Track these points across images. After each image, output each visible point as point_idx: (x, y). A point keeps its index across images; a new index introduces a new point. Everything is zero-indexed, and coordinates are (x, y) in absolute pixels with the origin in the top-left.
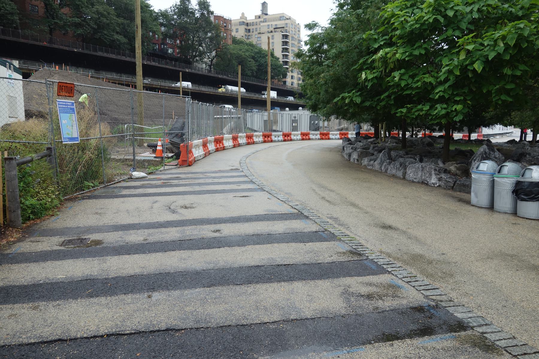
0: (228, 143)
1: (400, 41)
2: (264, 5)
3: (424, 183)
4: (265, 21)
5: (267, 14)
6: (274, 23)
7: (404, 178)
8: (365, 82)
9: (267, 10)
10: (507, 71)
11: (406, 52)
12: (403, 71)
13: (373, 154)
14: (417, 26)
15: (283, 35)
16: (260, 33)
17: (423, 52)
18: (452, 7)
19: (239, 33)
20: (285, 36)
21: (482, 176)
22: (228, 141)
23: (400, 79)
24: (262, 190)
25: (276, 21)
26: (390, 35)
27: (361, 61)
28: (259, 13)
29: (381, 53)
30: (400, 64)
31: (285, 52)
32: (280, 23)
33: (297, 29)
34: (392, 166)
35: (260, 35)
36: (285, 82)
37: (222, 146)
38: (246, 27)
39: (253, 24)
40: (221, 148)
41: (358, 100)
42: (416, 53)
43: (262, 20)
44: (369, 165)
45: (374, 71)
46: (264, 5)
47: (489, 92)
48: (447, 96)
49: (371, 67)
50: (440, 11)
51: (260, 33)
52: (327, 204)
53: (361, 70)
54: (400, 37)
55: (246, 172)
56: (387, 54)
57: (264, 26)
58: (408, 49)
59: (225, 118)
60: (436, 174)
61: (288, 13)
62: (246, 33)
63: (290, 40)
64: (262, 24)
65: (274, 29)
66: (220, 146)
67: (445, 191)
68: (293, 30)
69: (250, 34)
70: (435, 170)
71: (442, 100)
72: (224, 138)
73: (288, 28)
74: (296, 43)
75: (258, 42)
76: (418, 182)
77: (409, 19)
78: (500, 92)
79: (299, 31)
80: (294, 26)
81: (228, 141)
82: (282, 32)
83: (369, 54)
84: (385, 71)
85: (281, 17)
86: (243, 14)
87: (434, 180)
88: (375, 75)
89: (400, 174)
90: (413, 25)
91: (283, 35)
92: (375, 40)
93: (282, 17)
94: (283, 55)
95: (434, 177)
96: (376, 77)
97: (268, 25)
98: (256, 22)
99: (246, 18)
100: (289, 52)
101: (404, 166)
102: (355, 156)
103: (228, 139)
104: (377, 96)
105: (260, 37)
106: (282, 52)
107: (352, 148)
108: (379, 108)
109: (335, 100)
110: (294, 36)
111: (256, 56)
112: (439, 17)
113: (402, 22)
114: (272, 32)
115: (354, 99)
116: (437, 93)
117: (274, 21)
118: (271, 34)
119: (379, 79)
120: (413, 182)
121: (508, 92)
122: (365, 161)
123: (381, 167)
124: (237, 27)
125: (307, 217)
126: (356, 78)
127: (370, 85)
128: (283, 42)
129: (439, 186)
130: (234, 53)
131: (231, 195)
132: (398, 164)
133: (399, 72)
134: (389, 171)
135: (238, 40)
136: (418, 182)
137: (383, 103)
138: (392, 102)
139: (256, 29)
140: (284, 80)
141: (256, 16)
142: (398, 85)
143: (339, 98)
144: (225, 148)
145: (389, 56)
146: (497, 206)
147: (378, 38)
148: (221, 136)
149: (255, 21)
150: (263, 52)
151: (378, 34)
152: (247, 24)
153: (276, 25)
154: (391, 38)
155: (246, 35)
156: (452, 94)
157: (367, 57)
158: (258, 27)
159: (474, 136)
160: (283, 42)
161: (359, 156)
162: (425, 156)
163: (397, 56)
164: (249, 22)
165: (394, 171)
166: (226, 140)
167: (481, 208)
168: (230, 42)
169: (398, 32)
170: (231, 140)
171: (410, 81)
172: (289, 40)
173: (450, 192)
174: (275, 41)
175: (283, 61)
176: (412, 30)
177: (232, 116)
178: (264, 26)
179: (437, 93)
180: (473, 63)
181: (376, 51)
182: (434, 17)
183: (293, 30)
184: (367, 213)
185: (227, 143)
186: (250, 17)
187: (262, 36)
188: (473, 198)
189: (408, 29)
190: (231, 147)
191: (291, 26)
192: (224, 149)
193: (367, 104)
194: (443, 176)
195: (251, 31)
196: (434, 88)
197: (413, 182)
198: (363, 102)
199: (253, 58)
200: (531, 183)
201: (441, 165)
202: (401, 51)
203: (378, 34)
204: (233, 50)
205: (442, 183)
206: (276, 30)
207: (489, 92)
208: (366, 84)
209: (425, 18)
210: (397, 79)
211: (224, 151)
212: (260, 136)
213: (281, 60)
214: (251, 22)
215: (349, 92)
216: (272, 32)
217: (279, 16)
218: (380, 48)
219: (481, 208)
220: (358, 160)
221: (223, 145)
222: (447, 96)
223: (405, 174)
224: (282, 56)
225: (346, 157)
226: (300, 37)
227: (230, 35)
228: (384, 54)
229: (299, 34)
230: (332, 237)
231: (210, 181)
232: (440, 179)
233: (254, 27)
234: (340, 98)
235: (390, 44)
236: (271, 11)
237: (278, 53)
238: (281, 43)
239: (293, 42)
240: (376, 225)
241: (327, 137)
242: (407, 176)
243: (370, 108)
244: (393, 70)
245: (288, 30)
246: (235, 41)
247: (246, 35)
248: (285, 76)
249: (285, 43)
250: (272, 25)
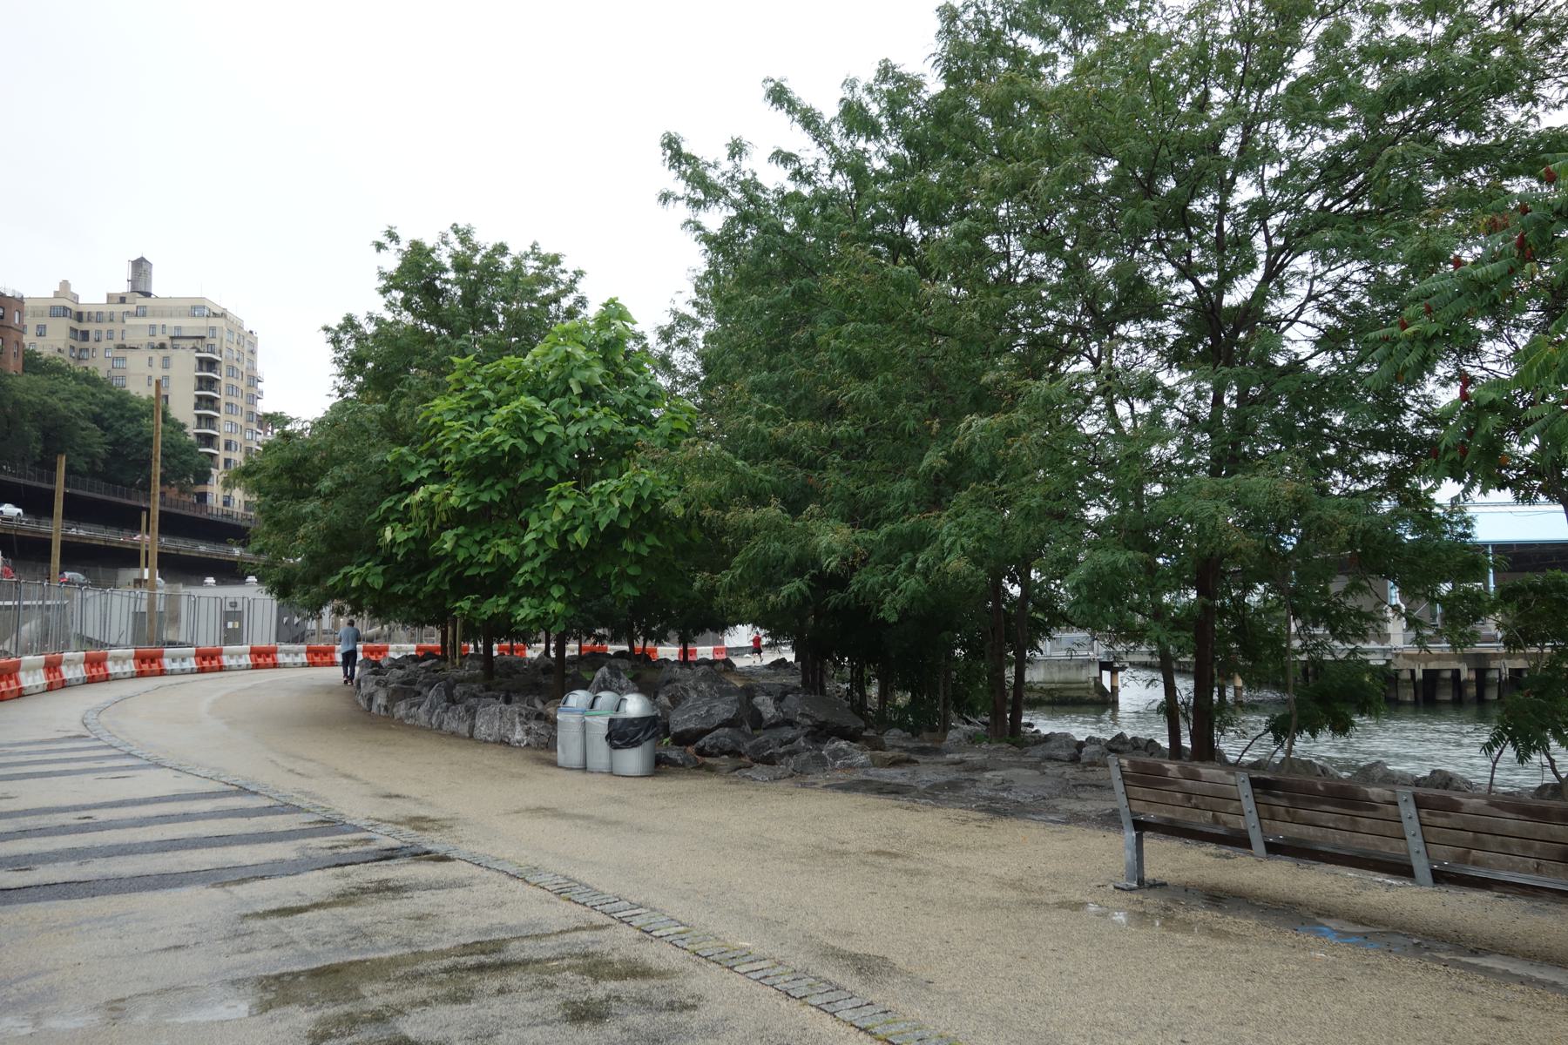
0: (32, 679)
1: (458, 473)
3: (504, 742)
4: (141, 313)
5: (148, 295)
6: (172, 323)
7: (471, 736)
8: (392, 547)
9: (148, 281)
10: (628, 545)
11: (467, 495)
12: (461, 530)
13: (419, 694)
14: (484, 450)
15: (201, 360)
16: (123, 347)
17: (497, 498)
18: (542, 427)
19: (52, 342)
20: (211, 364)
21: (569, 716)
22: (120, 662)
23: (457, 545)
24: (158, 765)
25: (180, 316)
26: (441, 460)
27: (385, 506)
28: (123, 287)
29: (420, 494)
30: (458, 517)
31: (206, 408)
32: (191, 325)
33: (247, 347)
34: (450, 714)
35: (121, 353)
36: (203, 497)
37: (14, 687)
38: (75, 324)
39: (99, 317)
40: (12, 691)
41: (377, 582)
42: (485, 497)
43: (132, 308)
44: (408, 717)
45: (410, 526)
47: (607, 577)
48: (536, 583)
49: (404, 518)
50: (522, 431)
51: (123, 347)
52: (297, 777)
53: (384, 521)
54: (458, 466)
55: (107, 740)
56: (432, 494)
58: (472, 490)
59: (26, 607)
60: (522, 723)
61: (220, 299)
62: (73, 343)
63: (224, 374)
64: (130, 321)
65: (172, 338)
66: (8, 686)
67: (530, 752)
68: (234, 347)
69: (90, 344)
70: (521, 715)
71: (528, 589)
72: (22, 665)
73: (216, 342)
74: (242, 385)
75: (115, 373)
76: (495, 742)
77: (471, 437)
78: (622, 576)
79: (252, 352)
80: (236, 337)
81: (120, 662)
82: (199, 351)
83: (400, 490)
84: (431, 526)
85: (194, 308)
86: (65, 285)
87: (518, 735)
88: (412, 534)
89: (464, 729)
90: (477, 447)
91: (201, 360)
92: (412, 467)
93: (197, 309)
94: (199, 417)
95: (518, 728)
96: (413, 538)
97: (153, 327)
98: (112, 314)
99: (77, 297)
100: (218, 410)
101: (472, 712)
102: (381, 699)
103: (32, 669)
104: (419, 572)
105: (124, 359)
106: (197, 407)
107: (378, 683)
108: (421, 596)
109: (331, 582)
110: (236, 364)
111: (106, 415)
112: (520, 442)
113: (457, 440)
114: (162, 346)
115: (369, 580)
116: (522, 575)
117: (171, 316)
118: (162, 352)
119: (422, 542)
120: (486, 741)
121: (632, 580)
122: (401, 709)
123: (430, 719)
124: (41, 321)
125: (256, 793)
126: (375, 535)
127: (401, 552)
128: (200, 379)
129: (528, 745)
130: (29, 401)
131: (90, 777)
132: (461, 708)
133: (455, 531)
134: (445, 727)
135: (46, 362)
136: (495, 742)
137: (428, 589)
138: (447, 587)
139: (110, 332)
140: (200, 488)
141: (110, 297)
142: (451, 556)
143: (337, 578)
144: (24, 692)
145: (436, 499)
146: (589, 765)
147: (418, 462)
148: (14, 659)
150: (132, 405)
151: (420, 455)
152: (79, 317)
153: (178, 328)
154: (443, 465)
155: (72, 348)
156: (547, 578)
157: (395, 498)
159: (704, 651)
160: (200, 379)
161: (389, 699)
162: (515, 692)
163: (452, 500)
164: (85, 310)
165: (454, 725)
166: (27, 670)
167: (572, 769)
168: (13, 365)
169: (451, 458)
170: (42, 672)
171: (475, 550)
172: (221, 376)
173: (542, 753)
174: (172, 372)
175: (198, 435)
176: (476, 457)
177: (48, 603)
179: (522, 575)
180: (575, 529)
181: (412, 488)
182: (512, 441)
183: (234, 347)
184: (367, 783)
185: (30, 679)
186: (91, 295)
187: (129, 354)
188: (561, 756)
189: (469, 455)
190: (40, 690)
191: (226, 336)
192: (64, 687)
193: (398, 589)
194: (533, 725)
195: (92, 336)
196: (517, 565)
197: (486, 741)
198: (387, 585)
199: (97, 419)
200: (625, 720)
201: (540, 706)
202: (458, 492)
203: (420, 455)
204: (27, 391)
205: (531, 739)
206: (176, 342)
207: (607, 577)
208: (394, 551)
209: (497, 440)
210: (448, 546)
211: (63, 690)
212: (190, 656)
213: (192, 430)
214: (94, 310)
215: (361, 565)
216: (162, 346)
217: (188, 304)
218: (420, 482)
219: (572, 769)
220: (386, 708)
221: (18, 683)
222: (536, 583)
223: (472, 728)
224: (195, 419)
225: (363, 704)
226: (254, 369)
227: (18, 343)
228: (426, 495)
229: (252, 362)
230: (298, 809)
231: (23, 758)
232: (528, 732)
234: (340, 576)
235: (440, 476)
236: (162, 286)
237: (183, 408)
238: (193, 383)
239: (234, 382)
240: (375, 795)
241: (327, 659)
242: (476, 732)
243: (405, 596)
244: (442, 528)
245: (217, 346)
246: (32, 363)
247: (72, 348)
248: (204, 477)
249: (207, 383)
250: (164, 326)
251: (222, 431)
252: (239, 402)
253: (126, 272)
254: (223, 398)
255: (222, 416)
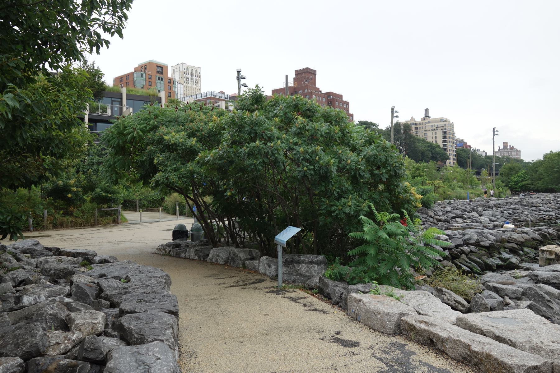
2: (427, 110)
4: (429, 122)
5: (429, 117)
6: (436, 124)
9: (429, 114)
16: (426, 131)
35: (426, 132)
46: (427, 110)
51: (426, 131)
57: (429, 127)
61: (445, 116)
64: (427, 125)
69: (418, 130)
74: (451, 136)
79: (453, 127)
93: (441, 120)
97: (432, 125)
114: (434, 130)
141: (421, 119)
149: (421, 122)
152: (416, 124)
153: (438, 125)
158: (424, 126)
172: (448, 135)
178: (429, 127)
195: (419, 128)
216: (434, 130)
229: (453, 130)
233: (421, 126)
239: (450, 136)
249: (445, 137)
251: (448, 147)
252: (451, 140)
253: (424, 112)
254: (448, 140)
255: (448, 144)
